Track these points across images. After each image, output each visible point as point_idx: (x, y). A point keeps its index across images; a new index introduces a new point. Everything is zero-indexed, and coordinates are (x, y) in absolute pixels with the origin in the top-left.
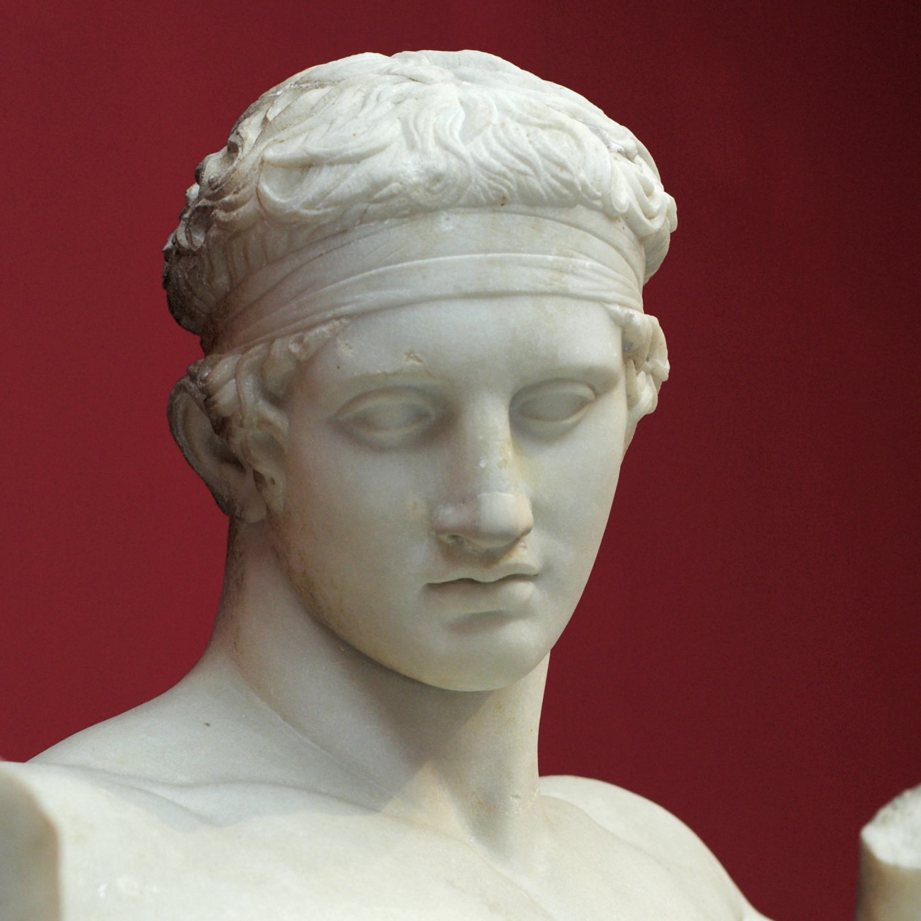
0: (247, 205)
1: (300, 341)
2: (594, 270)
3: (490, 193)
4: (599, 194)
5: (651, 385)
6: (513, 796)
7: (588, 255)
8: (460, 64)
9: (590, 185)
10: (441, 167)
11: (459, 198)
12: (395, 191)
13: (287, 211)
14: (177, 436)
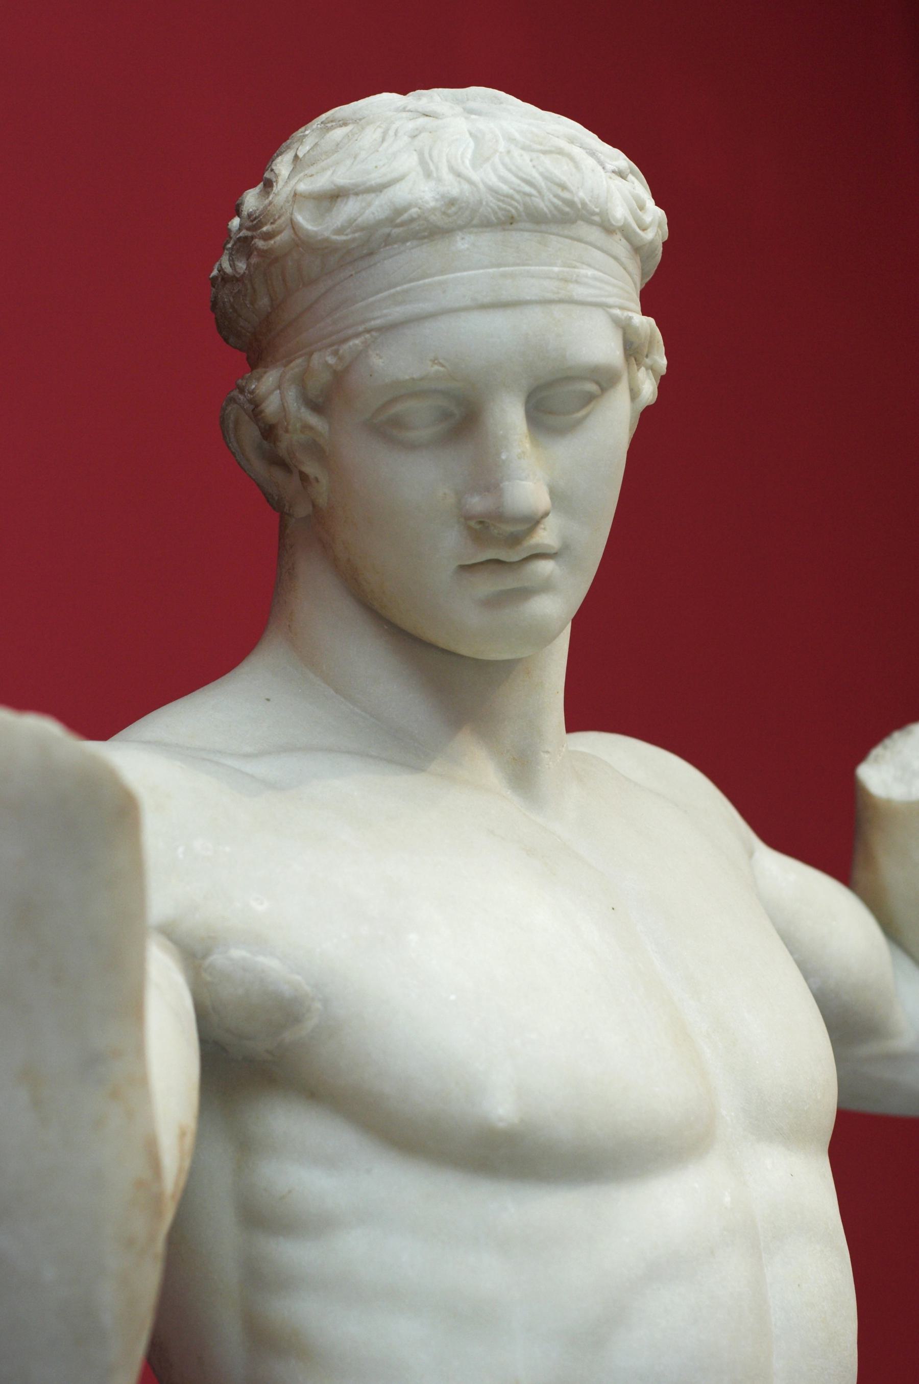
0: (283, 234)
1: (336, 353)
2: (595, 278)
3: (500, 214)
4: (597, 210)
5: (651, 379)
6: (544, 752)
7: (589, 265)
8: (468, 100)
9: (588, 203)
10: (455, 192)
11: (472, 220)
12: (415, 216)
13: (319, 238)
14: (230, 443)
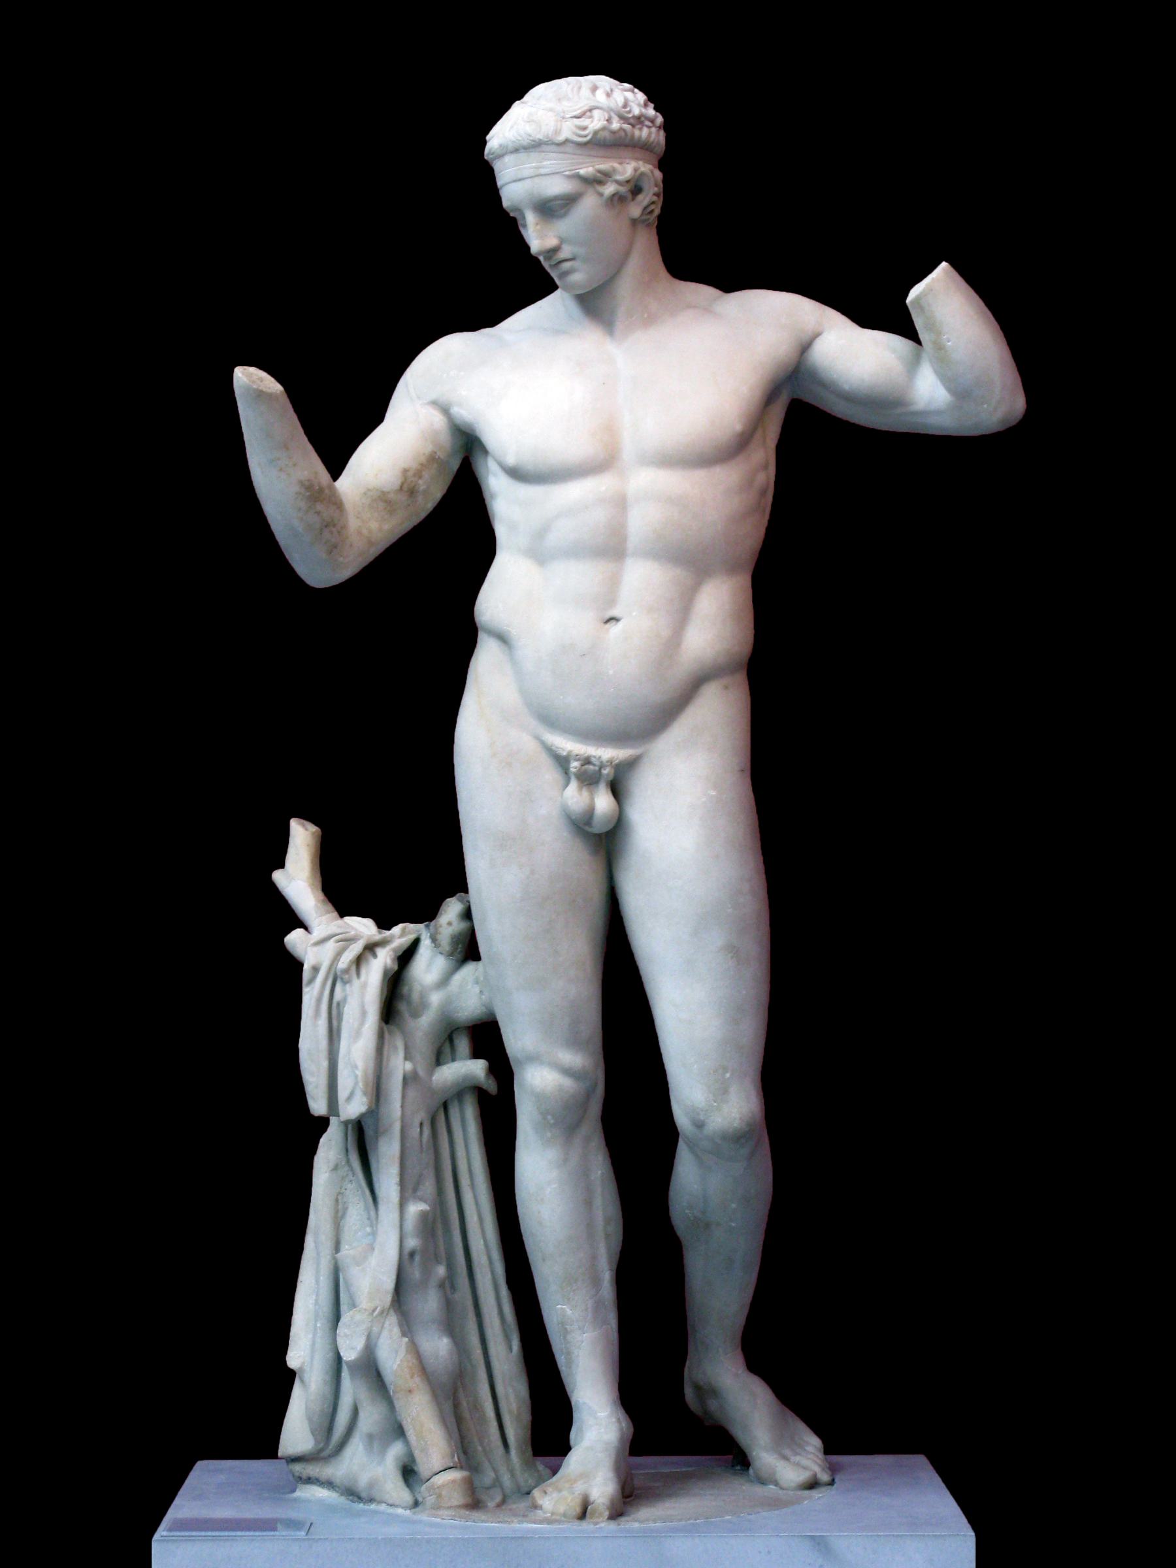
2: (551, 164)
